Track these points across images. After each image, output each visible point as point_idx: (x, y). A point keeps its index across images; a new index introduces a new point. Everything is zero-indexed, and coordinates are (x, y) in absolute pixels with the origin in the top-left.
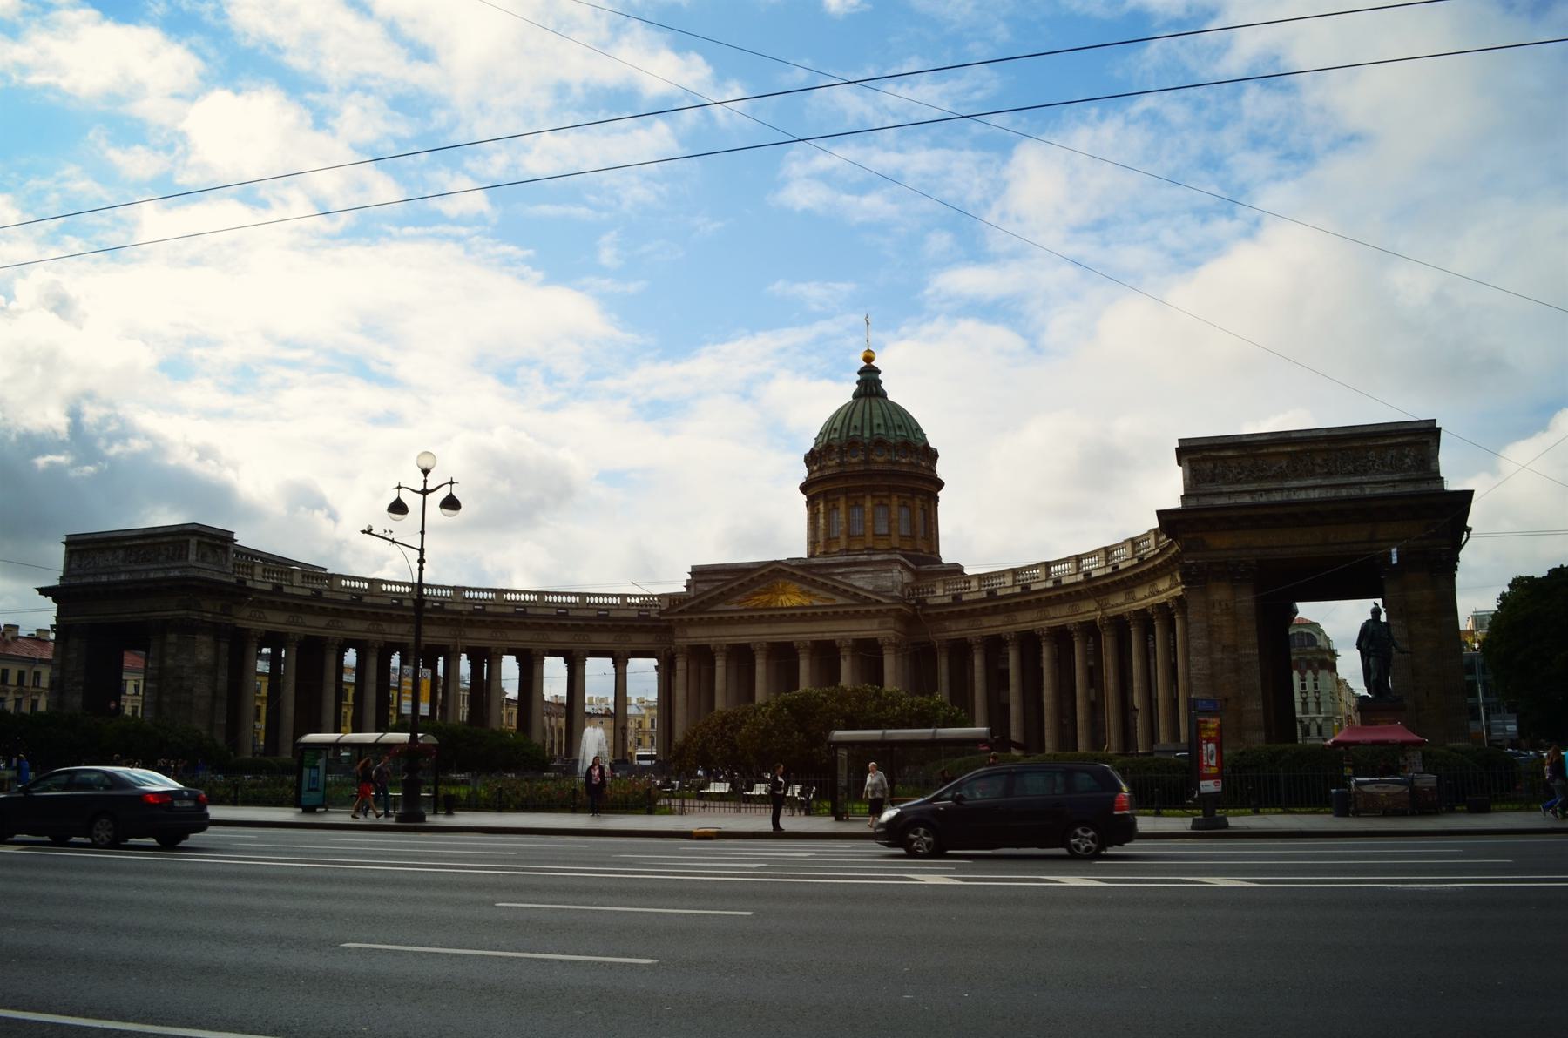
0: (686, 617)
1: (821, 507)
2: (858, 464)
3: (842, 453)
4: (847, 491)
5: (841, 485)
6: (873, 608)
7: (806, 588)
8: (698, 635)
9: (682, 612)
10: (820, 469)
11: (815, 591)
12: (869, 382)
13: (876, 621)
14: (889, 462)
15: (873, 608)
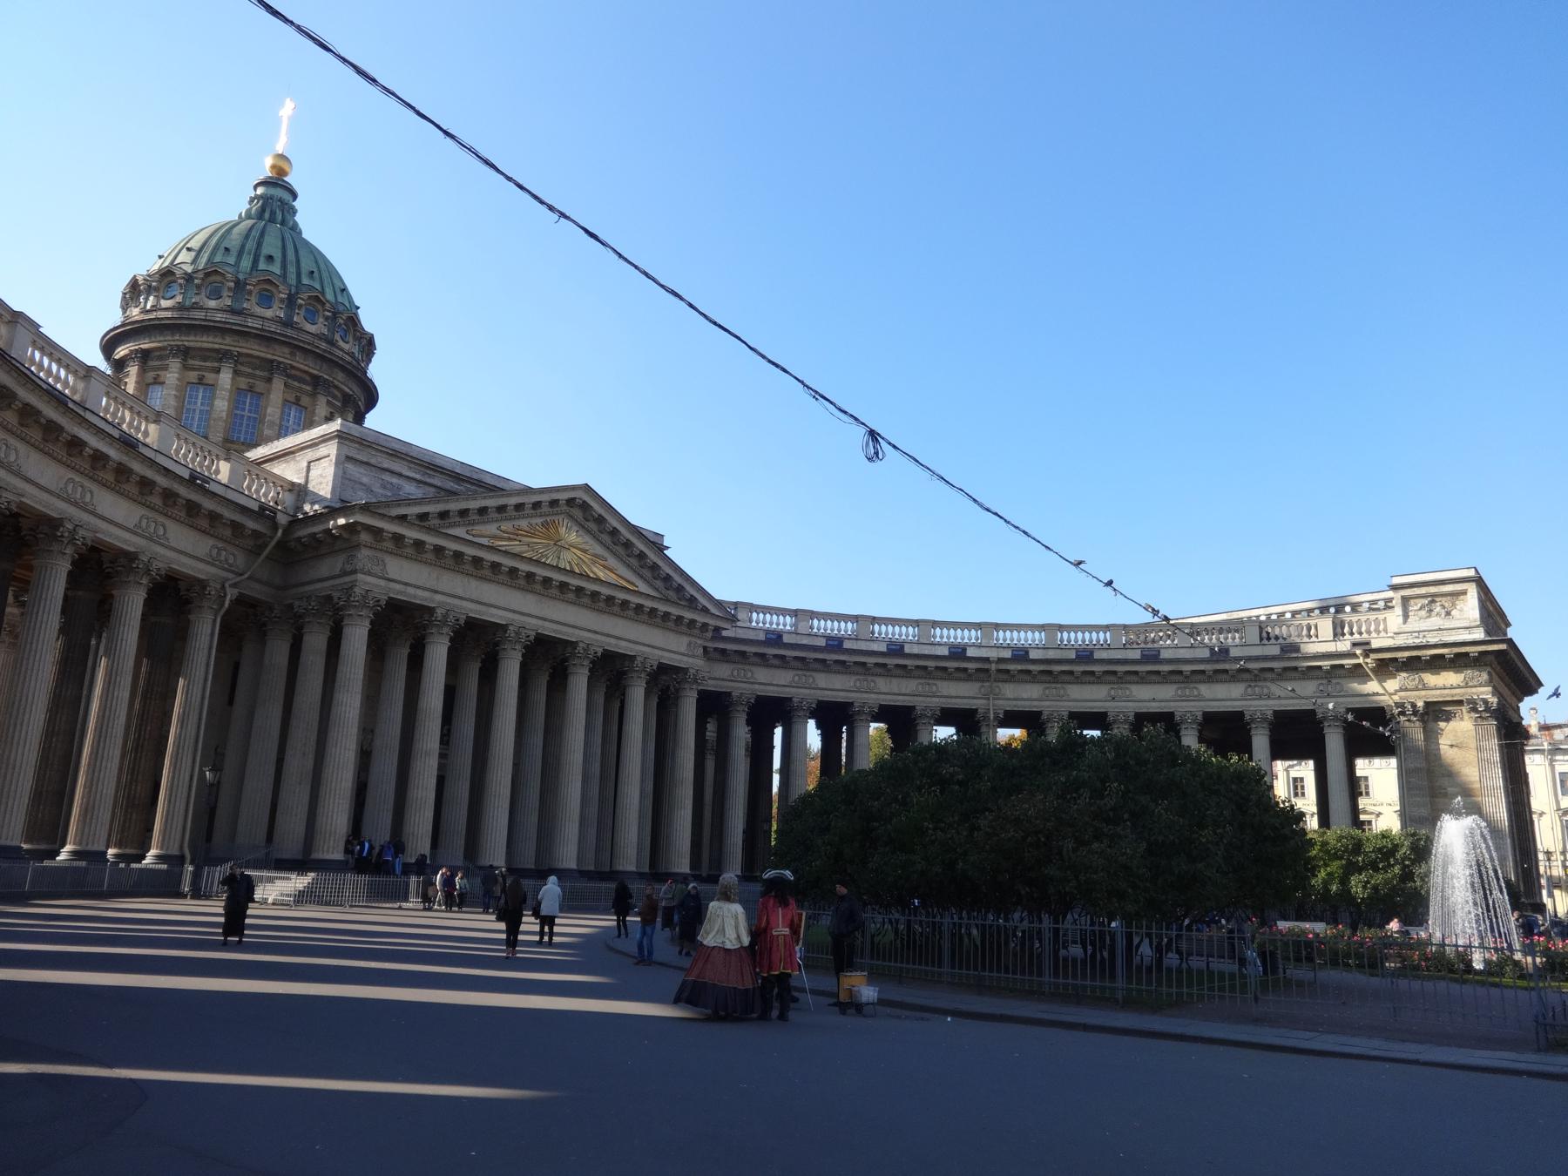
0: (411, 534)
1: (225, 378)
2: (320, 337)
3: (291, 302)
4: (287, 371)
5: (280, 355)
6: (700, 619)
7: (599, 550)
8: (409, 579)
9: (403, 518)
10: (232, 311)
11: (612, 562)
12: (276, 200)
13: (685, 640)
14: (351, 354)
15: (700, 619)
